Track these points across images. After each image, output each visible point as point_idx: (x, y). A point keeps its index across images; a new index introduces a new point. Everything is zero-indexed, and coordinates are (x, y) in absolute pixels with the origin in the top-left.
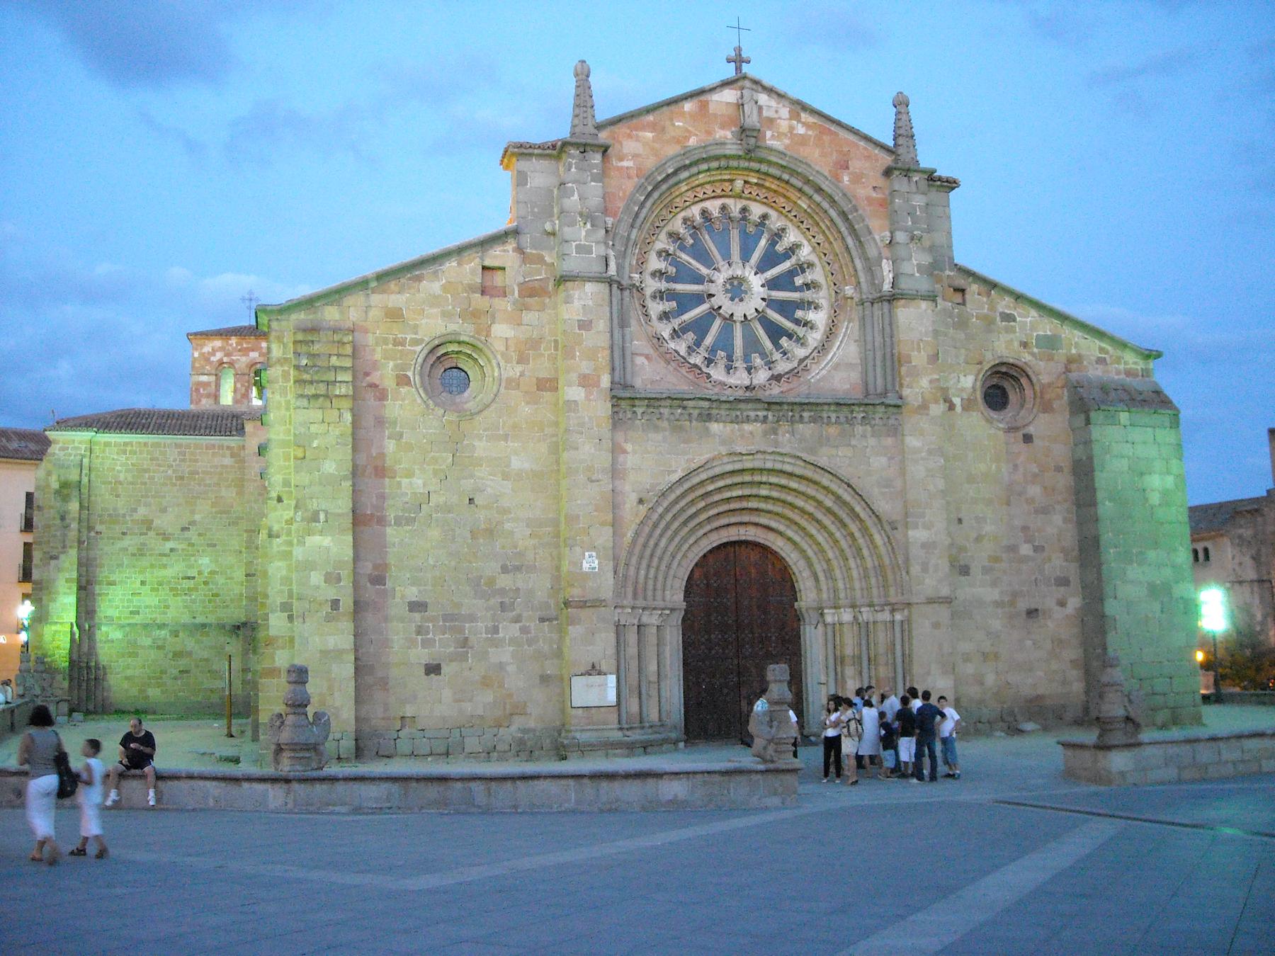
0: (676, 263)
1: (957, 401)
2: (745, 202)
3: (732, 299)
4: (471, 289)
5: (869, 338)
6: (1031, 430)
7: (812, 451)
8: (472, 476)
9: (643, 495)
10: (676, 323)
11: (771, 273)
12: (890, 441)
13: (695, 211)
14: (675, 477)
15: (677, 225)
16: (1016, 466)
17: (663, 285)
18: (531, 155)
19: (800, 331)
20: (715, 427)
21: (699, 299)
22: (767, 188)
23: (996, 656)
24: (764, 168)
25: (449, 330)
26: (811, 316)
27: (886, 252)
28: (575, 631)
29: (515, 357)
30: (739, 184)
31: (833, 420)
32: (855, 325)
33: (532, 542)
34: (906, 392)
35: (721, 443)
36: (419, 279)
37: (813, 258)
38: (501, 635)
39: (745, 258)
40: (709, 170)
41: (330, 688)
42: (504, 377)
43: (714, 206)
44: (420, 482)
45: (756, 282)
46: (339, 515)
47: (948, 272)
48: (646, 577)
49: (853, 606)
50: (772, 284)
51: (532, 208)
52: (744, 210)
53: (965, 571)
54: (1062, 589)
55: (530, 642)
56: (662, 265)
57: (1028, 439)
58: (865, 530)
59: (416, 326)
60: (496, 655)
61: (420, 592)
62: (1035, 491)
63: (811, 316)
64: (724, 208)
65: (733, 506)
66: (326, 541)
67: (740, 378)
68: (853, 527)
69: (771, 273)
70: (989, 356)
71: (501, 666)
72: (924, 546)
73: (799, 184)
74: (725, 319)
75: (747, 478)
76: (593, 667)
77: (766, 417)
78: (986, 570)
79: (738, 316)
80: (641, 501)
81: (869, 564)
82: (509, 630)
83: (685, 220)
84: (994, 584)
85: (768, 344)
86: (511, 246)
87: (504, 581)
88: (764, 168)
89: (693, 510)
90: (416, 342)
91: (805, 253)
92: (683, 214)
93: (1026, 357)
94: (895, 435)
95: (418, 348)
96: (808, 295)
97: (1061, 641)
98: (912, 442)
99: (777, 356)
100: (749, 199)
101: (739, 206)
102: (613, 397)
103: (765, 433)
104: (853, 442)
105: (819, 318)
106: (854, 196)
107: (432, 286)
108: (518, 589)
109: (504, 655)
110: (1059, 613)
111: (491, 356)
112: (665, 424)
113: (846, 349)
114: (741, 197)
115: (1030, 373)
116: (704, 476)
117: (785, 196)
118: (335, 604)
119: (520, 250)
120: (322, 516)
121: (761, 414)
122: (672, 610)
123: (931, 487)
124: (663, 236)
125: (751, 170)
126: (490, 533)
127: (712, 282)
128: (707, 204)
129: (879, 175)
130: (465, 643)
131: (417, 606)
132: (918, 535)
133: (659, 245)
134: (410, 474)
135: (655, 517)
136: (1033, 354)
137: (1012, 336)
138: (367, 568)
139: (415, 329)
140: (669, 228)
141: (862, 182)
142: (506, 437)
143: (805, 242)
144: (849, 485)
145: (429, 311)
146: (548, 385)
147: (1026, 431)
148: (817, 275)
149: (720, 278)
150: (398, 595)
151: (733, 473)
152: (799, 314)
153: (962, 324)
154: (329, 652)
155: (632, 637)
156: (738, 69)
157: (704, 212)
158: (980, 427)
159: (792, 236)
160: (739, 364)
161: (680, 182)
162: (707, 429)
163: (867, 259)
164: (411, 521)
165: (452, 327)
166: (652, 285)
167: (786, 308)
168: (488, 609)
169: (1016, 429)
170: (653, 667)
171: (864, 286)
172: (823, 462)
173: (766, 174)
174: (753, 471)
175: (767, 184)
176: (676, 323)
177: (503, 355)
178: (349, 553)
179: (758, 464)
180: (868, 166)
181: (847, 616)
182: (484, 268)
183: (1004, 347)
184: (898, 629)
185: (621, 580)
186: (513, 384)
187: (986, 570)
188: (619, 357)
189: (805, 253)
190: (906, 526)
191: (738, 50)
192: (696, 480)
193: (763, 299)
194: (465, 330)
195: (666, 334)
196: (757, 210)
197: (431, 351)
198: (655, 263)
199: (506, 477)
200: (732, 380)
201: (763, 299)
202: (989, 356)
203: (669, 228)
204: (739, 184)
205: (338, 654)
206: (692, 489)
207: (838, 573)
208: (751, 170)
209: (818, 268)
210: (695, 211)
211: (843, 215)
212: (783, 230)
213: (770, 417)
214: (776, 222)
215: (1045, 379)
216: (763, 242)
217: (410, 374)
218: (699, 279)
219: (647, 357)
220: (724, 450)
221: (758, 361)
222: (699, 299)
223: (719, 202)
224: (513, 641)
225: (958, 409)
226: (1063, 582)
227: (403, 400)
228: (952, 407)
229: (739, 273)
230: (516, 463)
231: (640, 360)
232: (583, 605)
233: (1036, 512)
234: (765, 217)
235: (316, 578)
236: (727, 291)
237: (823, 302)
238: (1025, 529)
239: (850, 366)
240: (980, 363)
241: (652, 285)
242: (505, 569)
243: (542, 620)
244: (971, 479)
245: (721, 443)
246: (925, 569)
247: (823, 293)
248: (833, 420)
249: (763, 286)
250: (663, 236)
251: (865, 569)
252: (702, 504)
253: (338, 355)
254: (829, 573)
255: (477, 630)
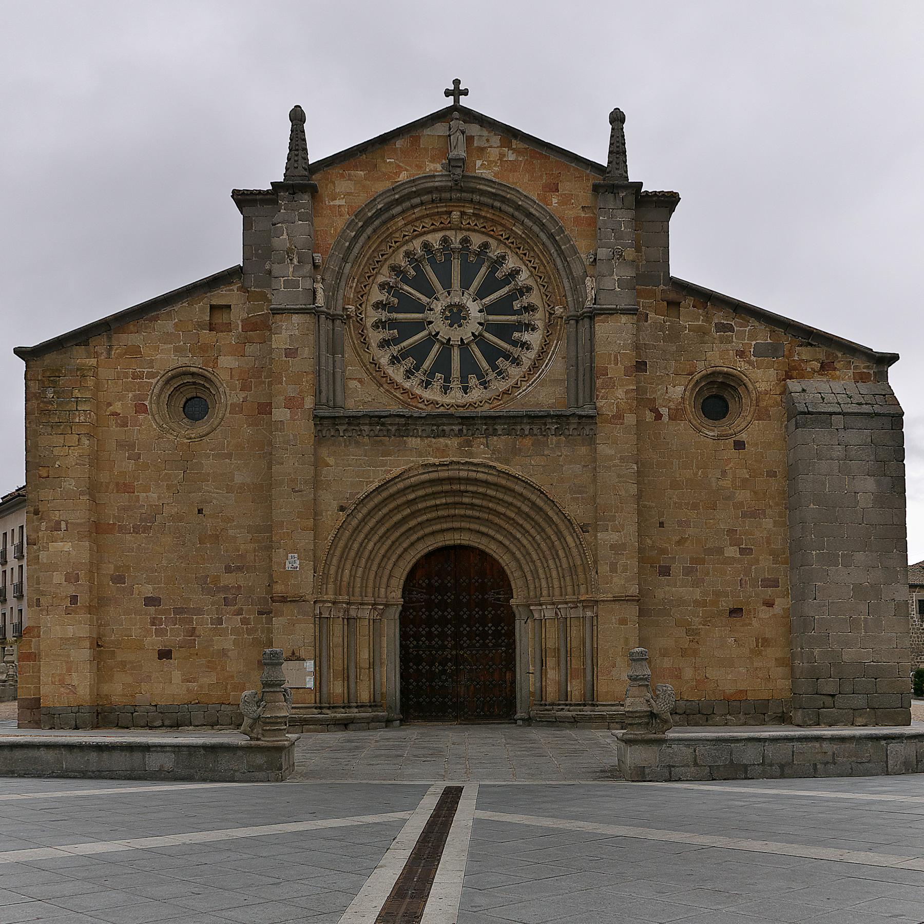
0: (398, 293)
1: (664, 411)
2: (465, 233)
3: (451, 325)
4: (200, 326)
5: (573, 354)
6: (743, 436)
7: (507, 462)
8: (200, 489)
9: (343, 502)
10: (395, 350)
11: (487, 301)
12: (583, 450)
13: (417, 244)
14: (373, 487)
15: (400, 259)
16: (724, 473)
17: (384, 315)
18: (255, 201)
19: (516, 351)
20: (413, 442)
21: (419, 326)
22: (485, 218)
23: (695, 653)
24: (476, 197)
25: (180, 364)
26: (526, 337)
27: (590, 271)
28: (278, 622)
29: (239, 386)
30: (455, 215)
31: (527, 432)
32: (563, 344)
33: (252, 545)
34: (600, 403)
35: (416, 456)
36: (156, 319)
37: (531, 282)
38: (224, 625)
39: (465, 285)
40: (422, 204)
41: (69, 670)
42: (229, 403)
43: (434, 240)
44: (155, 495)
45: (474, 308)
46: (78, 524)
47: (662, 287)
48: (353, 576)
49: (553, 604)
50: (489, 310)
51: (256, 250)
52: (465, 240)
53: (665, 571)
54: (770, 591)
55: (249, 632)
56: (382, 297)
57: (739, 445)
58: (559, 534)
59: (152, 361)
60: (219, 643)
61: (154, 589)
62: (743, 495)
63: (526, 337)
64: (445, 240)
65: (440, 513)
66: (67, 547)
67: (456, 397)
68: (549, 530)
69: (487, 301)
70: (700, 365)
71: (224, 653)
72: (612, 547)
73: (511, 210)
74: (443, 343)
75: (447, 487)
76: (293, 653)
77: (461, 431)
78: (688, 572)
79: (455, 340)
80: (342, 509)
81: (565, 566)
82: (232, 622)
83: (407, 254)
84: (696, 584)
85: (484, 364)
86: (235, 287)
87: (228, 580)
88: (476, 197)
89: (399, 516)
90: (151, 375)
91: (524, 278)
92: (405, 248)
93: (742, 366)
94: (590, 445)
95: (154, 381)
96: (525, 318)
97: (765, 640)
98: (604, 449)
99: (492, 375)
100: (469, 230)
101: (460, 236)
102: (315, 417)
103: (460, 446)
104: (546, 453)
105: (534, 338)
106: (562, 218)
107: (165, 324)
108: (239, 587)
109: (227, 642)
110: (765, 613)
111: (219, 385)
112: (366, 440)
113: (555, 366)
114: (461, 229)
115: (746, 380)
116: (401, 486)
117: (501, 225)
118: (74, 599)
119: (244, 289)
120: (63, 526)
121: (456, 428)
122: (387, 605)
123: (623, 493)
124: (385, 270)
125: (465, 201)
126: (216, 538)
127: (431, 310)
128: (429, 238)
129: (589, 194)
130: (192, 632)
131: (151, 601)
132: (607, 537)
133: (381, 279)
134: (146, 489)
135: (355, 522)
136: (750, 363)
137: (729, 346)
138: (109, 569)
139: (152, 361)
140: (391, 262)
141: (568, 204)
142: (229, 456)
143: (524, 267)
144: (542, 493)
145: (162, 346)
146: (265, 409)
147: (737, 438)
148: (534, 298)
149: (438, 306)
150: (136, 591)
151: (432, 482)
152: (516, 335)
153: (674, 335)
154: (68, 639)
155: (338, 629)
156: (457, 101)
157: (426, 246)
158: (690, 436)
159: (511, 263)
160: (455, 384)
161: (393, 217)
162: (405, 442)
163: (573, 278)
164: (146, 529)
165: (186, 361)
166: (372, 316)
167: (503, 331)
168: (213, 604)
169: (727, 436)
170: (364, 655)
171: (571, 304)
172: (513, 471)
173: (479, 203)
174: (450, 480)
175: (483, 214)
176: (395, 350)
177: (227, 382)
178: (85, 557)
179: (451, 474)
180: (578, 190)
181: (549, 613)
182: (212, 307)
183: (717, 356)
184: (588, 625)
185: (322, 579)
186: (236, 408)
187: (688, 572)
188: (326, 380)
189: (524, 278)
190: (596, 530)
191: (457, 82)
192: (393, 490)
193: (480, 324)
194: (195, 363)
195: (384, 361)
196: (477, 240)
197: (168, 382)
198: (377, 295)
199: (230, 490)
200: (447, 400)
201: (480, 324)
202: (700, 365)
203: (391, 262)
204: (455, 215)
205: (76, 641)
206: (392, 497)
207: (542, 576)
208: (465, 201)
209: (535, 292)
210: (417, 244)
211: (551, 237)
212: (504, 258)
213: (465, 431)
214: (496, 251)
215: (762, 387)
216: (483, 270)
217: (146, 403)
218: (421, 308)
219: (360, 381)
220: (421, 461)
221: (473, 381)
222: (419, 326)
223: (440, 235)
224: (235, 631)
225: (665, 418)
226: (775, 583)
227: (140, 425)
228: (659, 416)
229: (457, 300)
230: (238, 479)
231: (353, 384)
232: (284, 600)
233: (744, 515)
234: (486, 245)
235: (58, 578)
236: (447, 318)
237: (539, 324)
238: (731, 532)
239: (556, 382)
240: (691, 374)
241: (372, 316)
242: (228, 569)
243: (260, 613)
244: (675, 485)
245: (416, 456)
246: (614, 568)
247: (539, 315)
248: (527, 432)
249: (480, 311)
250: (385, 270)
251: (563, 569)
252: (408, 511)
253: (82, 388)
254: (535, 574)
255: (204, 624)
